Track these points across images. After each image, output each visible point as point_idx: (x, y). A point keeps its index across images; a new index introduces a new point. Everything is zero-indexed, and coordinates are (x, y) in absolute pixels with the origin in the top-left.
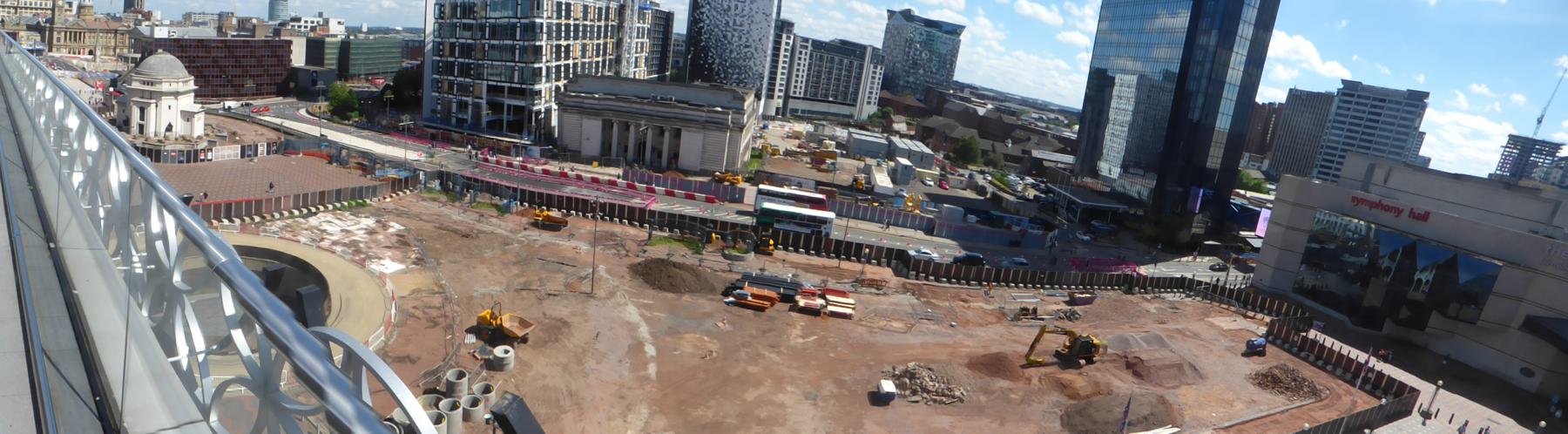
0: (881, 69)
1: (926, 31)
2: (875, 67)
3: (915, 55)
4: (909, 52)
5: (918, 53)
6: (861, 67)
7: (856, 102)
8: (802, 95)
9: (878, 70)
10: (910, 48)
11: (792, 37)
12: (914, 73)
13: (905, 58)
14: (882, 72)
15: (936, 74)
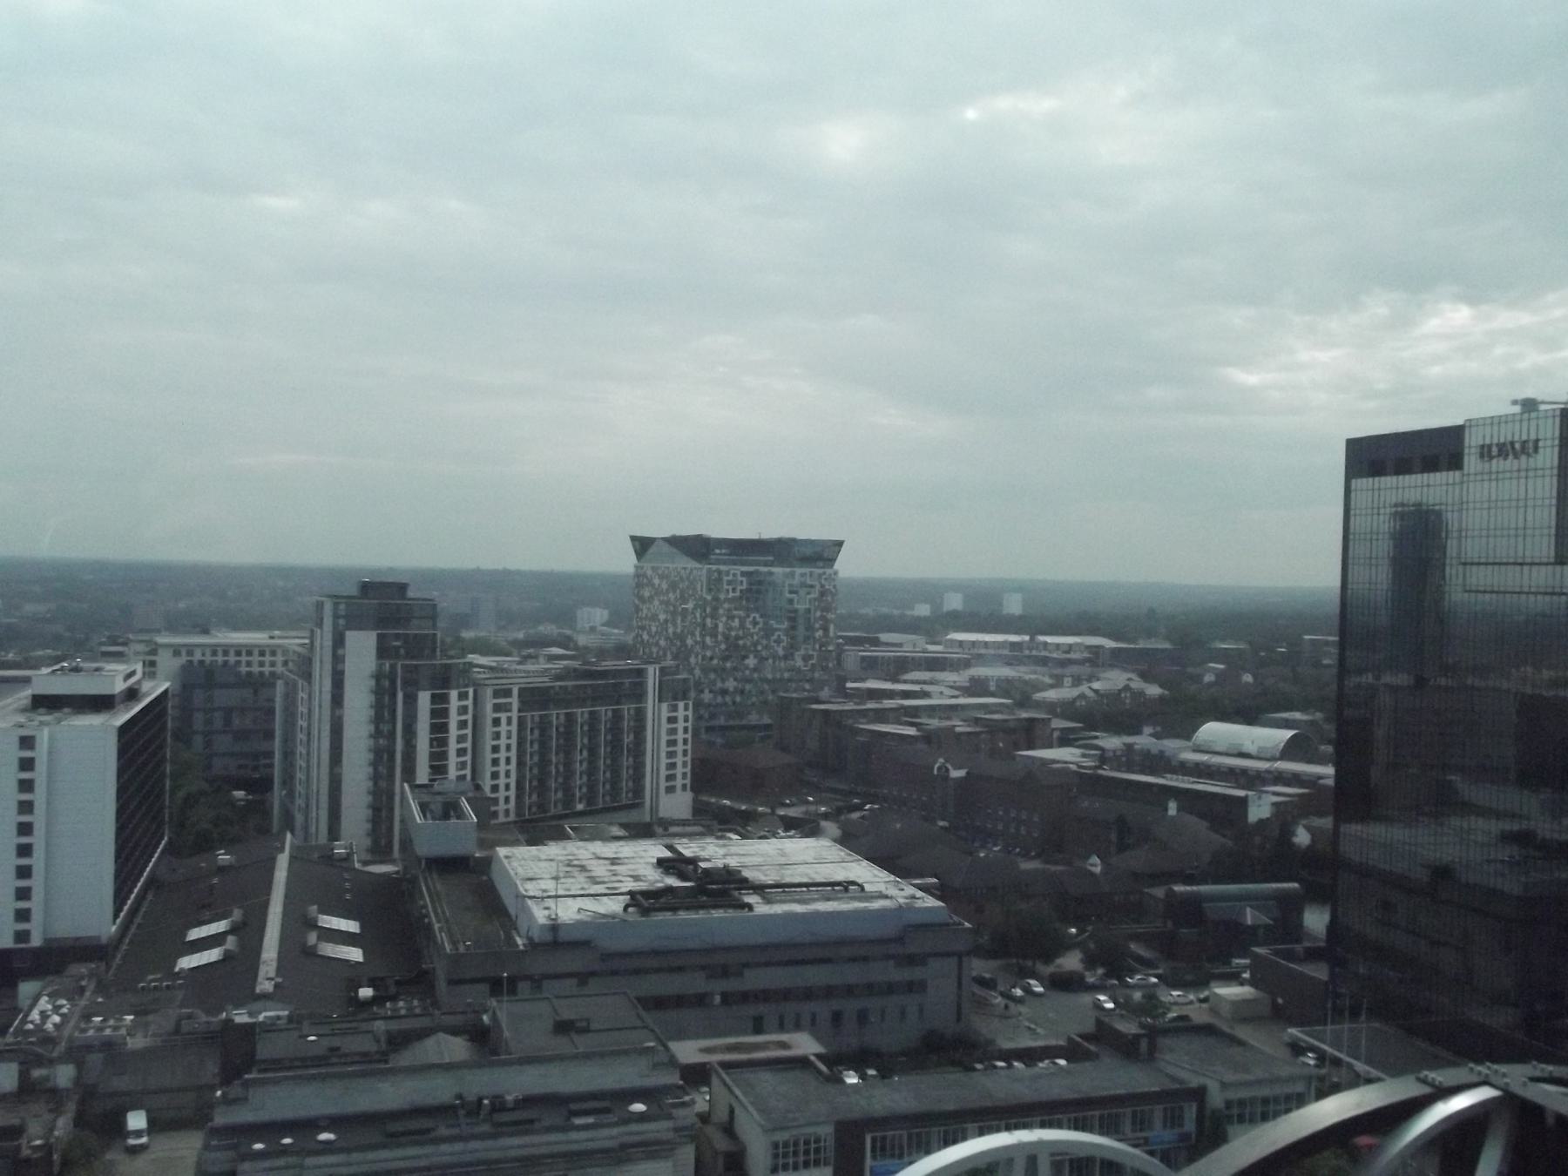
0: (686, 709)
1: (743, 574)
2: (674, 708)
3: (730, 629)
4: (716, 626)
5: (736, 623)
6: (640, 716)
7: (643, 797)
8: (512, 817)
9: (681, 714)
10: (714, 616)
11: (471, 691)
12: (735, 669)
13: (708, 639)
14: (690, 713)
15: (786, 658)
